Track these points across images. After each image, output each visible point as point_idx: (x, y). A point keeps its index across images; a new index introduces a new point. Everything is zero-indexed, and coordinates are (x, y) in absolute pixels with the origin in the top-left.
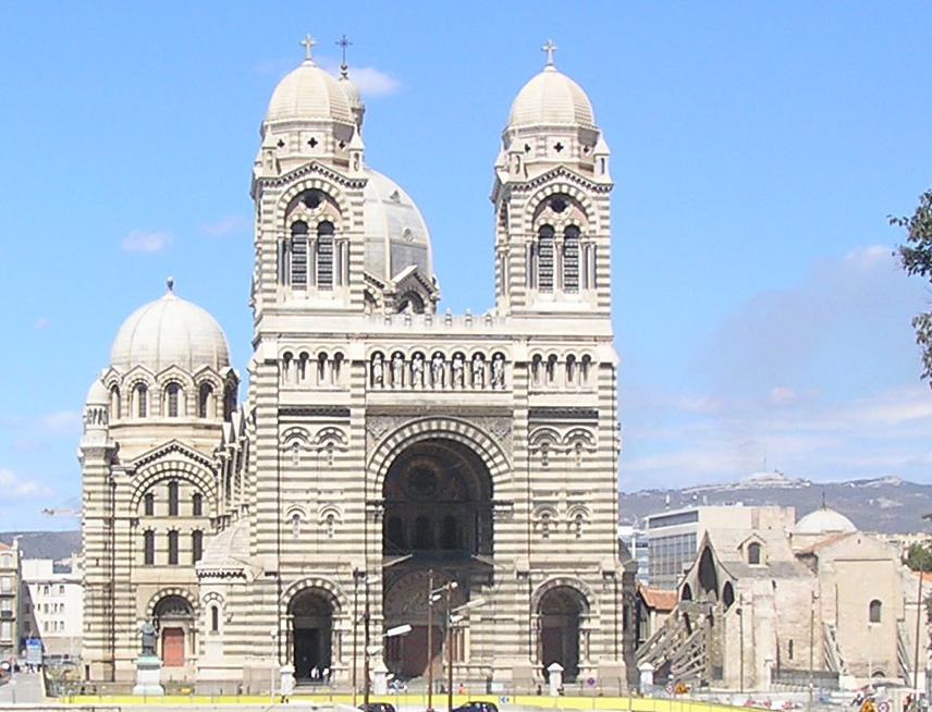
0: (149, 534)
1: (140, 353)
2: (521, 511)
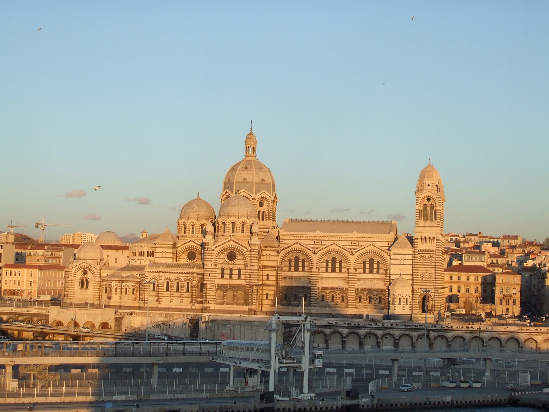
1: (250, 214)
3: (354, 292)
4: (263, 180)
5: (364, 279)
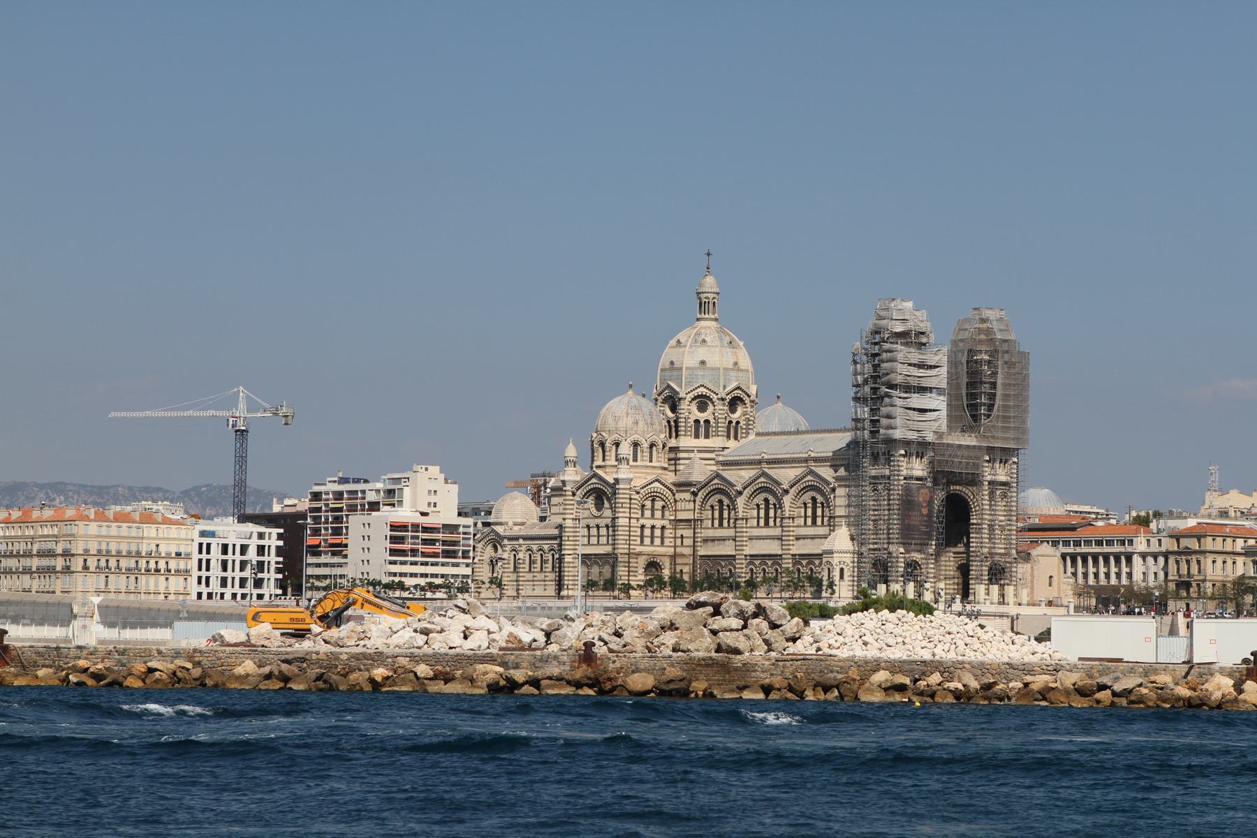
0: (643, 527)
2: (985, 529)
3: (790, 561)
4: (703, 362)
5: (804, 537)
